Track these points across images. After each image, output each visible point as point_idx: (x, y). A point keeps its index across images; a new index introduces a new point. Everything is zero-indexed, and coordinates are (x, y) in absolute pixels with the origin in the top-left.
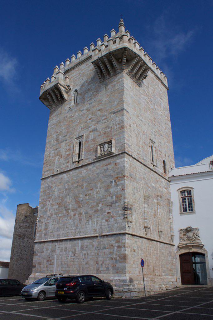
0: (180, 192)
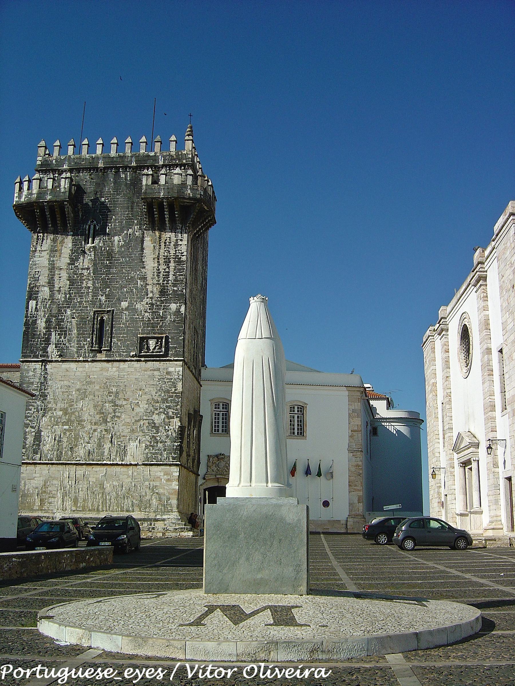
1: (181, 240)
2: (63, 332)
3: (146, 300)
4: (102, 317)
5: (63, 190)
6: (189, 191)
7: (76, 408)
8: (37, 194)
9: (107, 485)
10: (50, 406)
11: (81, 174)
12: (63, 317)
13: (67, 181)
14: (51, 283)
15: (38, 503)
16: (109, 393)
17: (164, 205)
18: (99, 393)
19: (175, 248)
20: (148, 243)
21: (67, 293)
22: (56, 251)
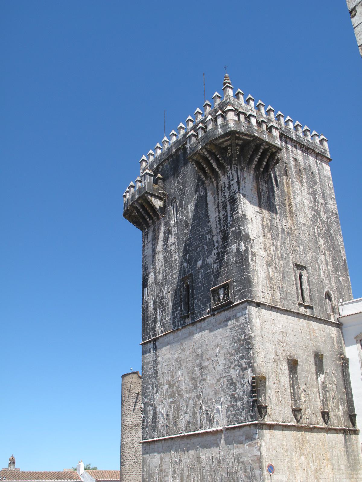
3: (214, 251)
6: (220, 130)
10: (160, 381)
16: (197, 356)
18: (191, 359)
20: (210, 198)
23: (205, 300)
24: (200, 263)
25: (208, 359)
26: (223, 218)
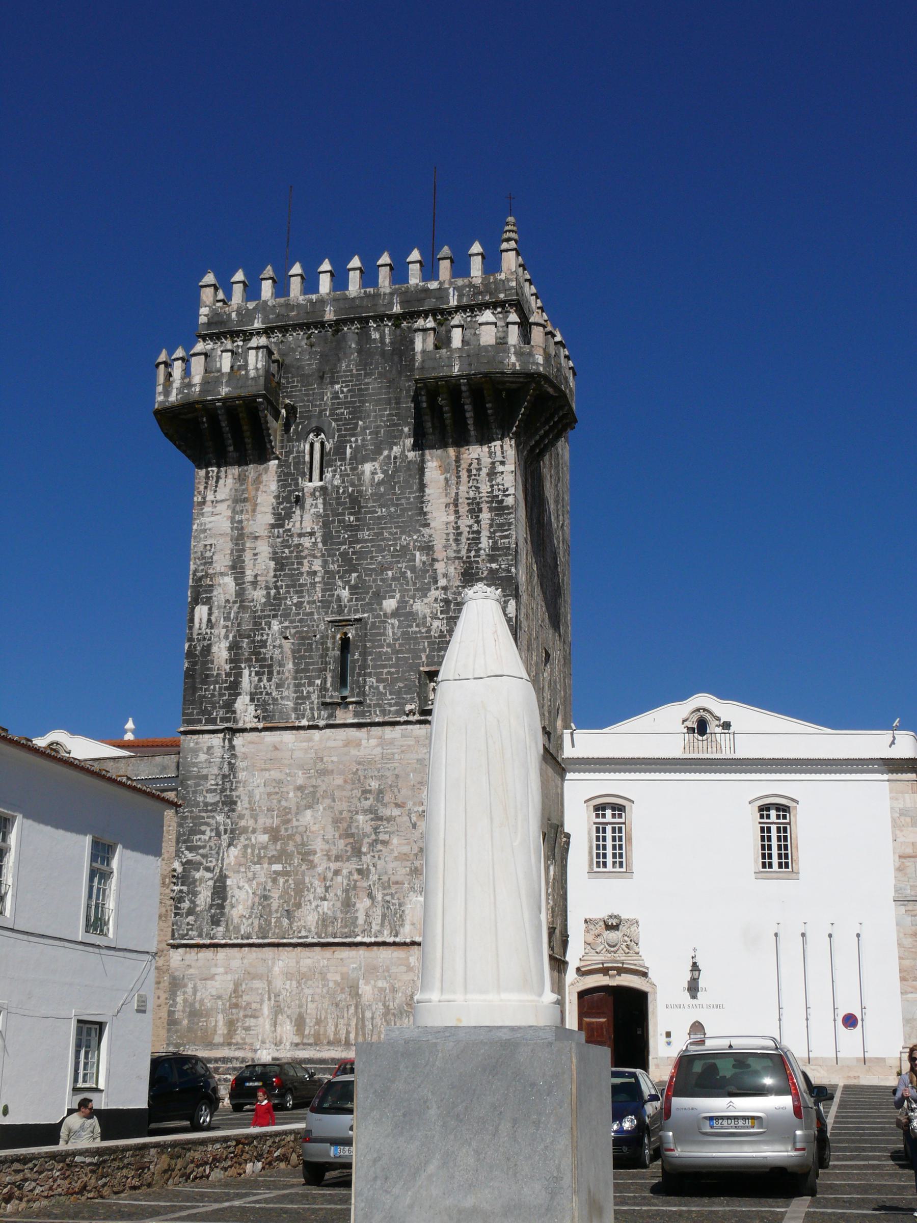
0: (592, 808)
1: (503, 463)
2: (266, 668)
3: (434, 593)
4: (346, 634)
5: (252, 373)
6: (513, 359)
7: (297, 827)
8: (202, 384)
9: (366, 990)
10: (243, 823)
11: (291, 338)
12: (265, 637)
13: (260, 355)
14: (237, 568)
15: (222, 1029)
16: (365, 792)
17: (461, 392)
18: (344, 793)
19: (491, 480)
21: (271, 585)
22: (245, 500)
23: (401, 685)
24: (390, 604)
25: (397, 805)
26: (469, 532)
